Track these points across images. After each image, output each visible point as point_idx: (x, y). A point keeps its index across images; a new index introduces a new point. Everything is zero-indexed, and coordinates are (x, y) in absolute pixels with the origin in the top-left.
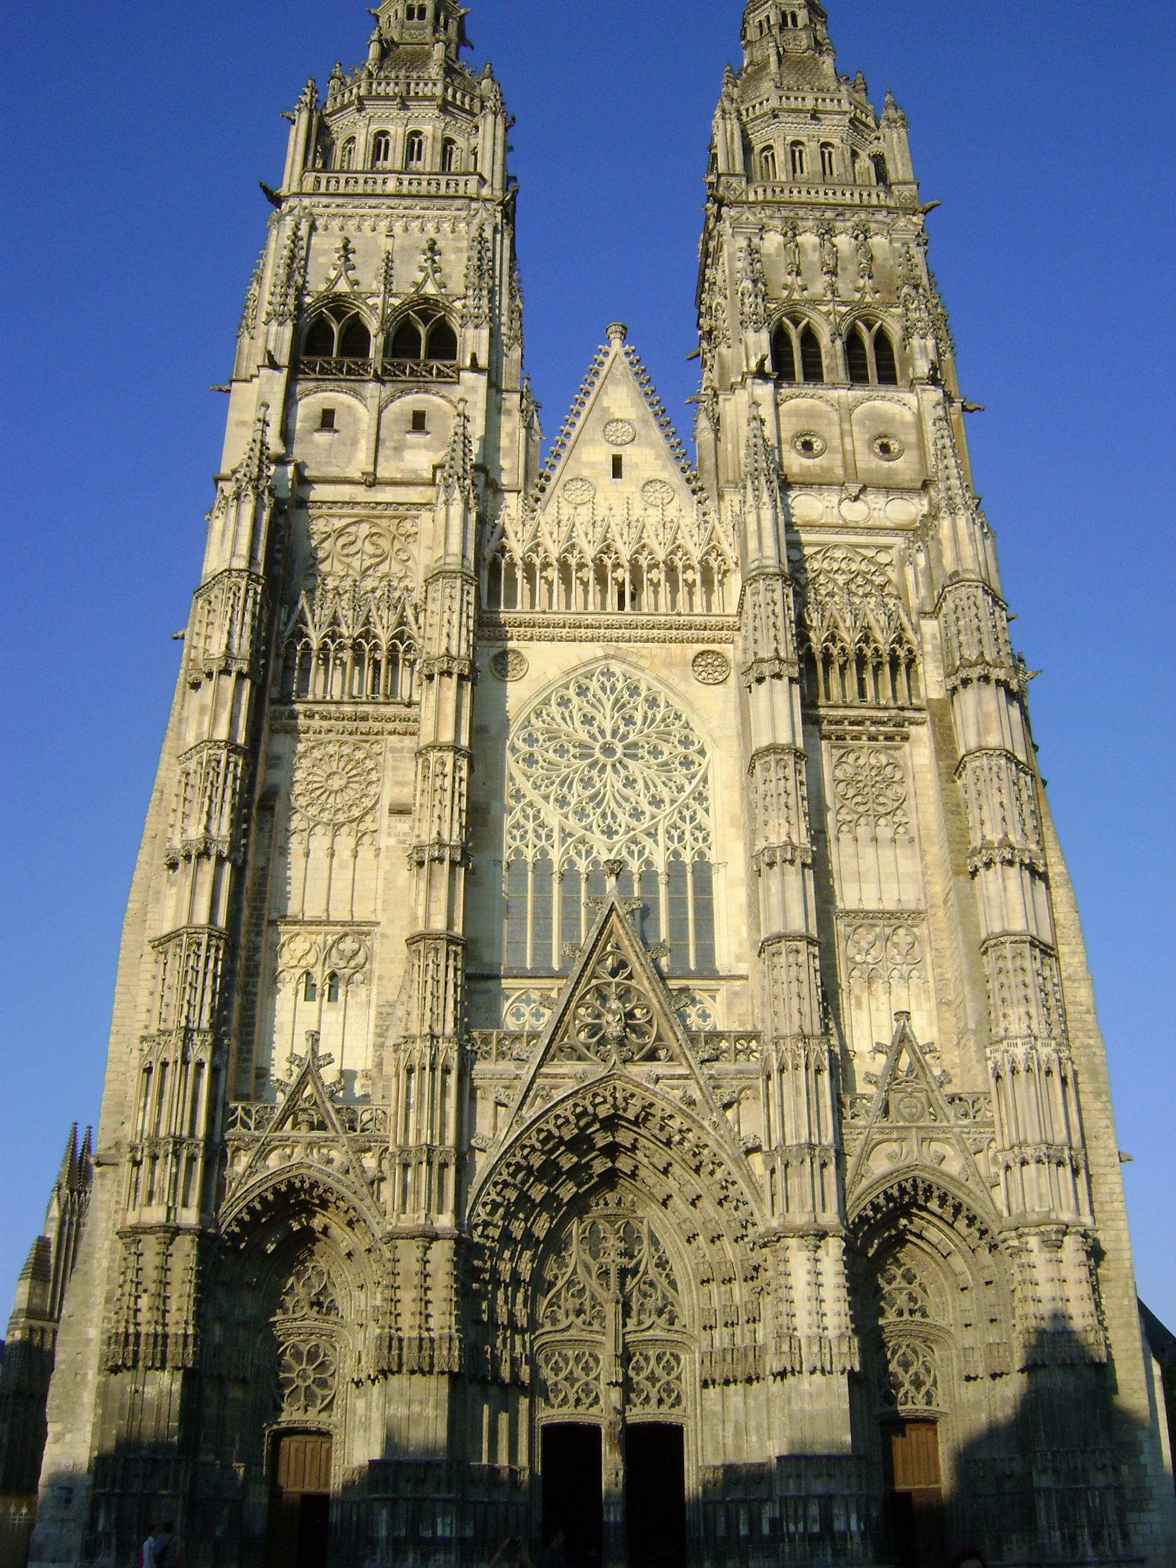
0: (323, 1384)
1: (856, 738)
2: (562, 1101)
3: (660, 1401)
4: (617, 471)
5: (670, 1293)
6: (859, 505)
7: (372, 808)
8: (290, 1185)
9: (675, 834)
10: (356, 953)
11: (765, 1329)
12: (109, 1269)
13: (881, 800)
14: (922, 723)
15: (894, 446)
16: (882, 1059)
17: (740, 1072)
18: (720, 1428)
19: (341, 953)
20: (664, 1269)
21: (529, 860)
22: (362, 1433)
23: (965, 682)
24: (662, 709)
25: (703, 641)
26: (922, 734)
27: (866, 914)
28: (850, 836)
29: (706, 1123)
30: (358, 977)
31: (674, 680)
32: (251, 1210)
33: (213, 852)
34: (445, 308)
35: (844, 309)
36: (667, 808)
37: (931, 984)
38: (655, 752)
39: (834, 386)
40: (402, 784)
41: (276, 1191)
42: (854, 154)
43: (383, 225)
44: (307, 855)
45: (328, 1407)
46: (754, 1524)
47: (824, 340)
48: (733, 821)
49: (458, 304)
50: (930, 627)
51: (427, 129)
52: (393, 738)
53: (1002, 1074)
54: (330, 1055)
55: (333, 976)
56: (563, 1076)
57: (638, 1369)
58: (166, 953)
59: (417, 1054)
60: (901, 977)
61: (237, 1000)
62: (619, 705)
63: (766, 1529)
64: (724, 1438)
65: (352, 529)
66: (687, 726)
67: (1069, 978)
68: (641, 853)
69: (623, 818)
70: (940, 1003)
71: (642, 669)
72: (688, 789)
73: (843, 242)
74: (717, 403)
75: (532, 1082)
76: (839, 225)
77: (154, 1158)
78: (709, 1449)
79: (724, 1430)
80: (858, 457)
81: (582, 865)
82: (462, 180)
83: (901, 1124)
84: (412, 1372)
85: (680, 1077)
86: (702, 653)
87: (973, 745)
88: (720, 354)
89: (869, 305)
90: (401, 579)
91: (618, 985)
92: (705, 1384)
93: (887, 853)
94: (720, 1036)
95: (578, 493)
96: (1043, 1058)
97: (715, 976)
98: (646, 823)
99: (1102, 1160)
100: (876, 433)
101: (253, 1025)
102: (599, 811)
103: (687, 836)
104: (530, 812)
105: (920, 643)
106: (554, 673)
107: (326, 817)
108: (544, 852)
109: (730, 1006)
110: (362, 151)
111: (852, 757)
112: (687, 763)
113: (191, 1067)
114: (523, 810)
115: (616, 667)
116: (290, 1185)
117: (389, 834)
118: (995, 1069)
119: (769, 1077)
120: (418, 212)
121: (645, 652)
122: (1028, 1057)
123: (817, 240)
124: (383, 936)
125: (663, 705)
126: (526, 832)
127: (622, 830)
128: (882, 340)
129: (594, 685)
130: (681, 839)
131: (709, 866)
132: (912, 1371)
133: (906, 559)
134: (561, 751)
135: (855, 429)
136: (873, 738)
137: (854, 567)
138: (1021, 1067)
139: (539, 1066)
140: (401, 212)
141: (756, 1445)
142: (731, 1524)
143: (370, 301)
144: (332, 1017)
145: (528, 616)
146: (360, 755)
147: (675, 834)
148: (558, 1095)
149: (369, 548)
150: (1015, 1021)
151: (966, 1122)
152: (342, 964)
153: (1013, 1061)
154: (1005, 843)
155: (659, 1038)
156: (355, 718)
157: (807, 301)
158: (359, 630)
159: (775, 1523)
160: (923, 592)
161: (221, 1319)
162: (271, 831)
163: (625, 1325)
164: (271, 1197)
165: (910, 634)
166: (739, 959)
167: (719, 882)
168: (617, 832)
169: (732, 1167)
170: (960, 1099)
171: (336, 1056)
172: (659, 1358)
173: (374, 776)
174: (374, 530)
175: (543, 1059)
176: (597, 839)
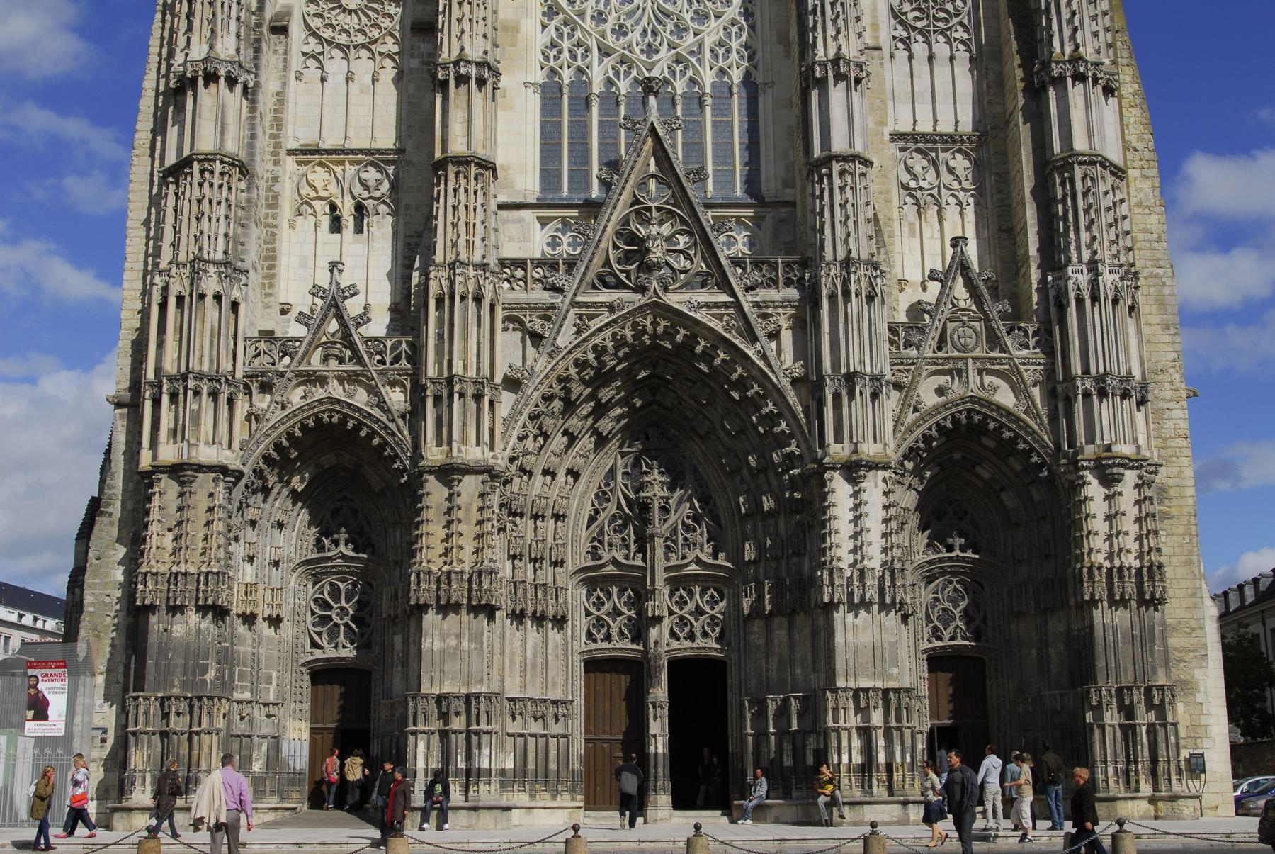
2: (600, 330)
8: (318, 420)
11: (810, 562)
12: (133, 510)
13: (942, 15)
16: (934, 287)
18: (763, 661)
19: (364, 184)
20: (707, 504)
21: (566, 81)
22: (400, 668)
28: (907, 53)
29: (750, 353)
32: (278, 447)
33: (222, 72)
36: (713, 23)
41: (304, 427)
44: (323, 80)
48: (784, 39)
53: (1065, 303)
54: (354, 286)
56: (603, 304)
59: (445, 283)
60: (960, 204)
64: (767, 670)
67: (1139, 205)
70: (1000, 230)
75: (568, 311)
79: (767, 663)
81: (624, 86)
83: (956, 354)
85: (725, 305)
91: (658, 209)
96: (1109, 285)
99: (1168, 394)
101: (274, 258)
102: (639, 29)
107: (343, 39)
113: (209, 300)
114: (557, 30)
116: (318, 420)
117: (412, 56)
118: (1057, 297)
119: (816, 305)
122: (1094, 284)
126: (560, 52)
139: (575, 294)
141: (801, 678)
148: (596, 324)
150: (1078, 247)
151: (1024, 352)
152: (366, 194)
153: (1079, 289)
154: (1076, 59)
161: (251, 559)
162: (286, 53)
163: (667, 559)
164: (298, 433)
166: (787, 183)
168: (657, 51)
170: (1020, 329)
171: (361, 287)
175: (578, 288)
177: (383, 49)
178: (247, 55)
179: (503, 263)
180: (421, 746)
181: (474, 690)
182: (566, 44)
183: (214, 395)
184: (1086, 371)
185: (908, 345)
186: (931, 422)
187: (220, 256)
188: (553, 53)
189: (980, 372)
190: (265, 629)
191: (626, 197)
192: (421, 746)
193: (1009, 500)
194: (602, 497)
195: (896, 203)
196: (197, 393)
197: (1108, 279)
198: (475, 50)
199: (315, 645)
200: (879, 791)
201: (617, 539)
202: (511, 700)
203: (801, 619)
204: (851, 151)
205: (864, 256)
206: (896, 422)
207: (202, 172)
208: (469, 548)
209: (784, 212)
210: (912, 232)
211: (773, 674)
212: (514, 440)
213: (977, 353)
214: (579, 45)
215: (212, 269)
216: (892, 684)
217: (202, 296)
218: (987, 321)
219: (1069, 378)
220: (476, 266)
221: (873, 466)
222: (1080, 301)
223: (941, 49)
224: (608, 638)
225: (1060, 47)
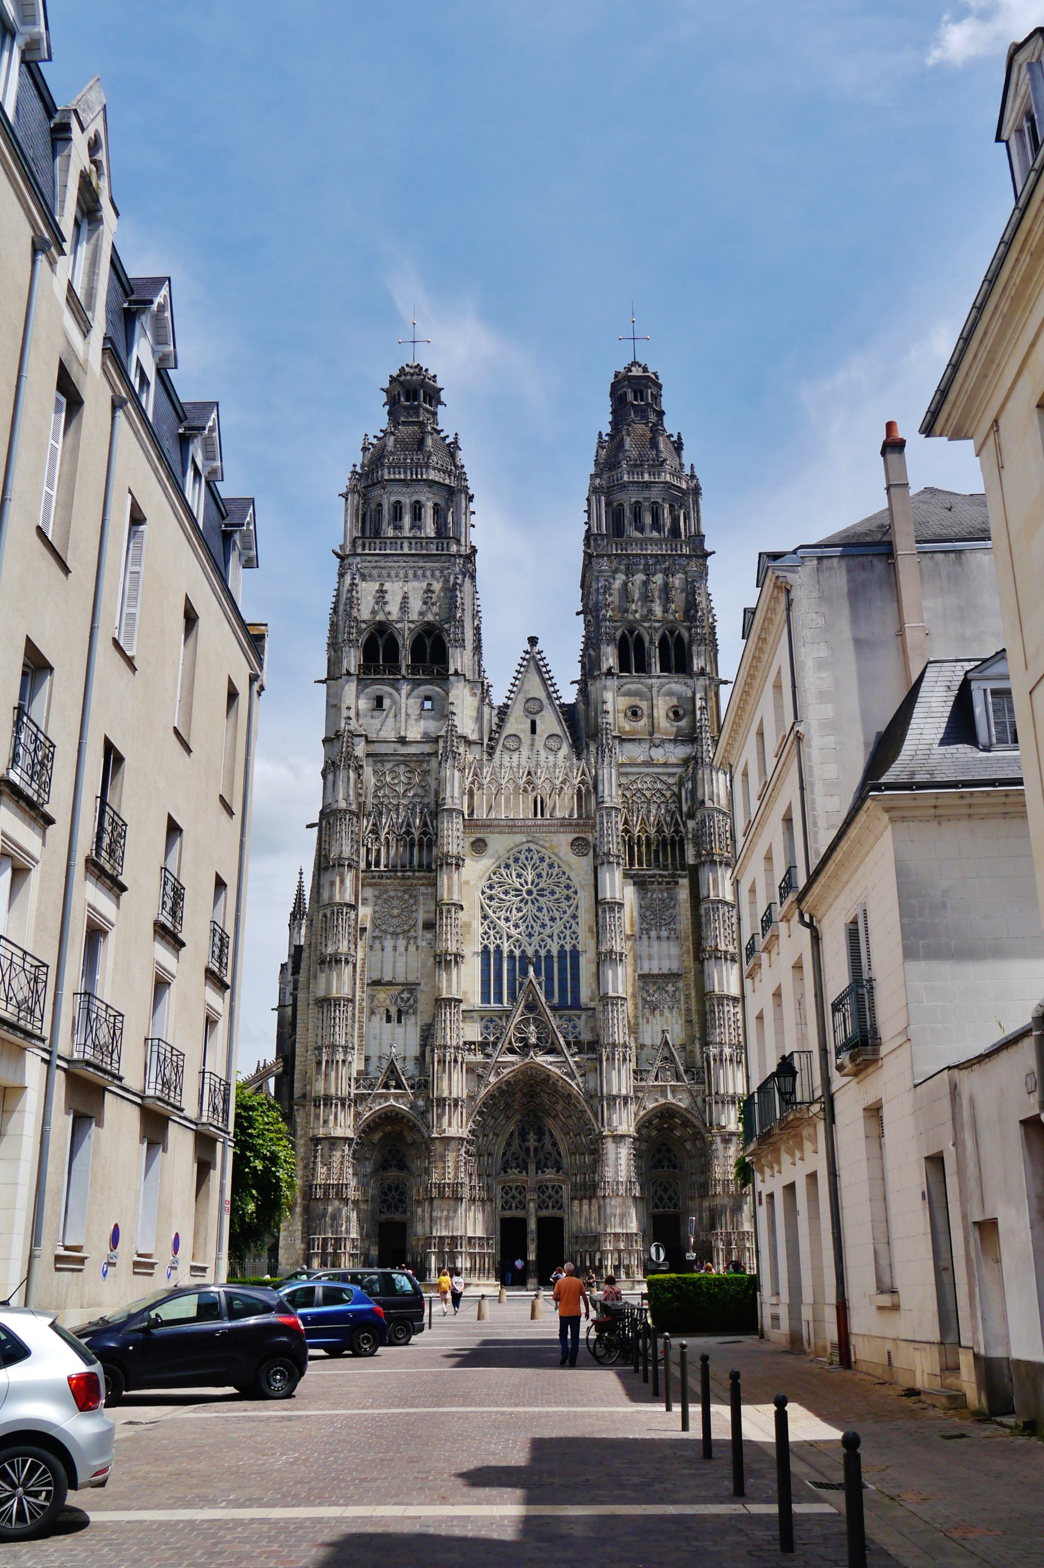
0: (402, 1201)
1: (652, 883)
3: (553, 1207)
4: (533, 731)
5: (558, 1157)
6: (660, 750)
7: (414, 925)
9: (562, 936)
10: (409, 999)
14: (685, 877)
15: (681, 712)
17: (588, 1059)
19: (402, 999)
23: (703, 863)
24: (556, 870)
25: (575, 832)
26: (684, 882)
27: (653, 976)
29: (573, 1084)
30: (411, 1011)
31: (561, 855)
32: (368, 1126)
34: (438, 628)
35: (657, 625)
37: (683, 1012)
38: (553, 893)
39: (650, 677)
40: (428, 912)
42: (671, 506)
43: (402, 573)
44: (383, 950)
45: (405, 1212)
46: (592, 1260)
47: (647, 644)
48: (590, 929)
49: (446, 626)
50: (691, 824)
51: (423, 499)
52: (423, 889)
55: (400, 1012)
57: (543, 1193)
58: (322, 1007)
61: (357, 1026)
62: (535, 867)
63: (597, 1263)
65: (396, 769)
66: (569, 878)
68: (545, 946)
69: (537, 928)
70: (686, 1021)
71: (545, 848)
72: (569, 912)
73: (659, 578)
74: (587, 685)
76: (658, 567)
77: (325, 1105)
78: (574, 1228)
80: (661, 720)
81: (517, 953)
82: (445, 541)
84: (443, 1198)
86: (576, 839)
87: (706, 895)
88: (589, 655)
89: (672, 622)
90: (422, 797)
92: (573, 1199)
93: (665, 944)
94: (580, 1042)
95: (512, 744)
97: (579, 1008)
98: (548, 931)
100: (671, 704)
102: (525, 925)
103: (568, 937)
104: (492, 926)
105: (687, 833)
106: (502, 851)
107: (391, 930)
108: (498, 946)
109: (586, 1023)
110: (387, 516)
111: (649, 894)
112: (568, 898)
115: (533, 847)
119: (601, 1062)
120: (421, 564)
121: (547, 839)
123: (644, 578)
124: (422, 991)
125: (556, 865)
127: (536, 934)
128: (680, 638)
129: (522, 857)
130: (565, 938)
131: (578, 952)
132: (668, 1193)
133: (681, 784)
134: (506, 893)
135: (660, 702)
136: (660, 883)
137: (655, 786)
138: (718, 1058)
140: (411, 564)
142: (583, 1261)
143: (398, 626)
144: (399, 1030)
145: (488, 822)
146: (406, 896)
147: (562, 936)
148: (506, 1071)
149: (406, 781)
154: (717, 950)
155: (553, 1043)
156: (403, 878)
157: (636, 621)
158: (404, 830)
159: (600, 1261)
160: (689, 803)
165: (682, 828)
166: (592, 1000)
167: (583, 960)
169: (584, 1103)
172: (553, 1187)
173: (414, 908)
174: (408, 769)
176: (524, 940)
177: (410, 935)
178: (353, 947)
179: (465, 1043)
180: (433, 1258)
181: (455, 1234)
182: (492, 932)
183: (343, 1105)
184: (717, 1093)
185: (641, 1080)
186: (650, 1114)
187: (343, 1043)
188: (485, 937)
189: (673, 1092)
190: (363, 1206)
191: (519, 1012)
192: (433, 1258)
193: (688, 1146)
194: (508, 1144)
195: (640, 1008)
196: (336, 1105)
197: (727, 1051)
198: (452, 948)
199: (381, 1212)
200: (623, 1276)
201: (514, 1165)
202: (470, 1238)
203: (594, 1201)
204: (616, 995)
205: (622, 1041)
206: (636, 1114)
207: (335, 1005)
208: (453, 1173)
209: (590, 1013)
210: (648, 1022)
211: (583, 1225)
212: (470, 1123)
213: (672, 1083)
214: (498, 933)
215: (341, 1049)
216: (629, 1231)
217: (337, 1062)
218: (676, 1068)
219: (710, 1095)
220: (455, 1048)
221: (622, 1137)
222: (715, 1060)
223: (664, 934)
224: (511, 1208)
225: (709, 944)
